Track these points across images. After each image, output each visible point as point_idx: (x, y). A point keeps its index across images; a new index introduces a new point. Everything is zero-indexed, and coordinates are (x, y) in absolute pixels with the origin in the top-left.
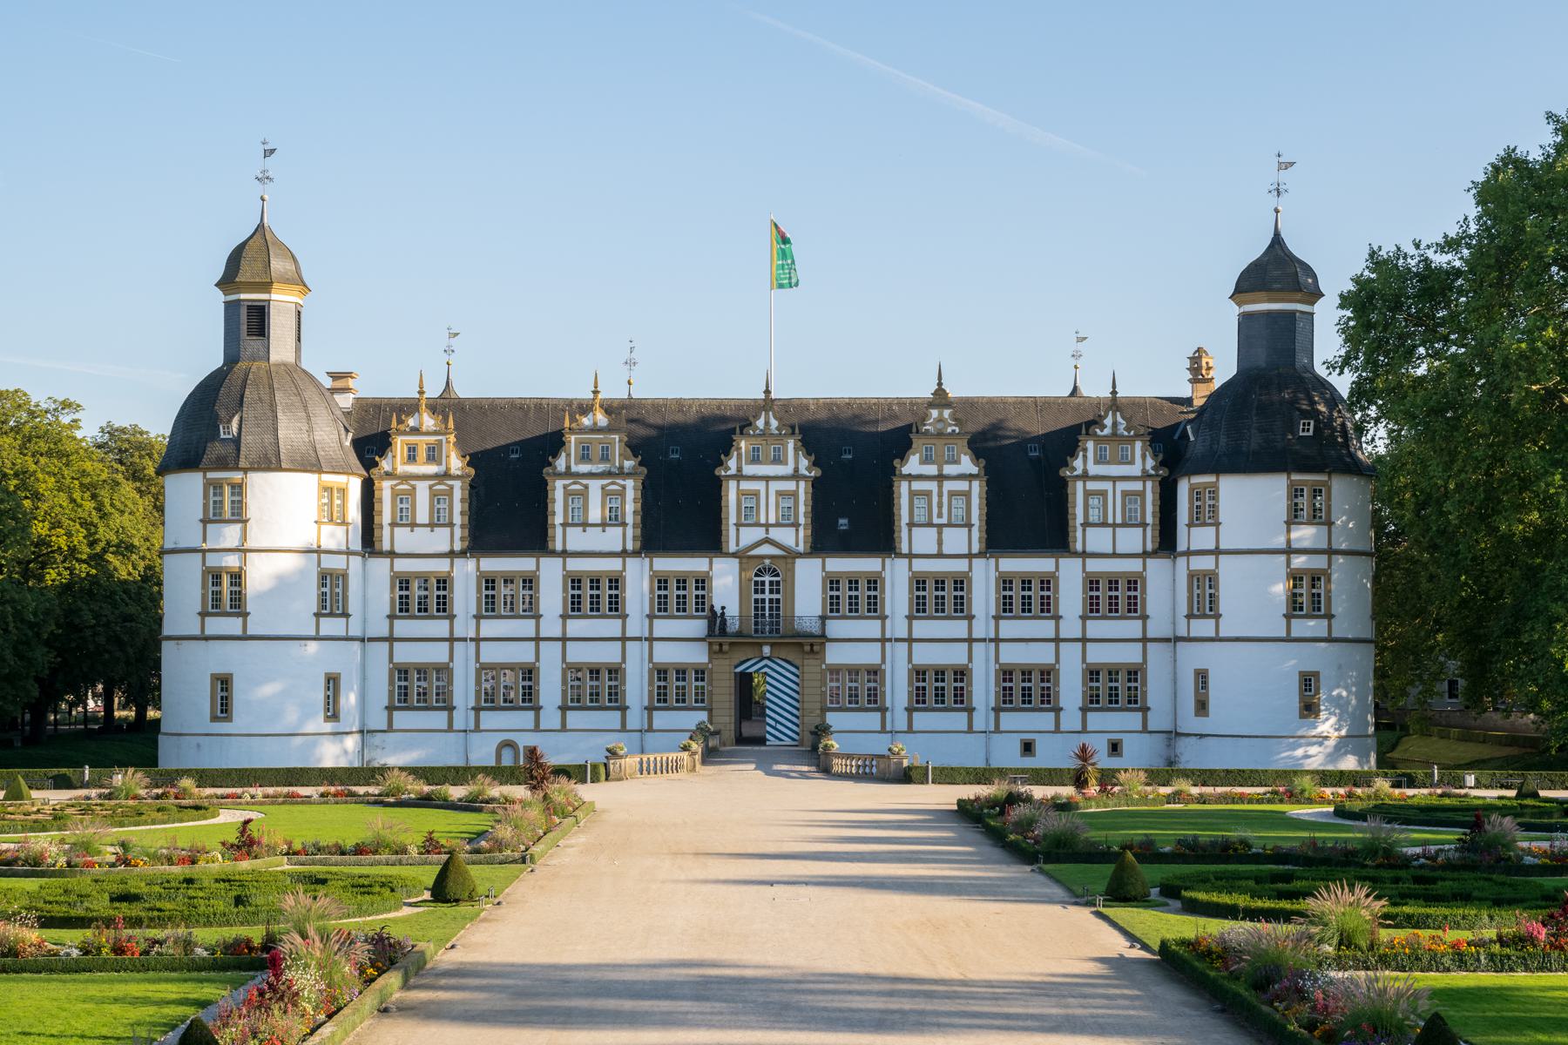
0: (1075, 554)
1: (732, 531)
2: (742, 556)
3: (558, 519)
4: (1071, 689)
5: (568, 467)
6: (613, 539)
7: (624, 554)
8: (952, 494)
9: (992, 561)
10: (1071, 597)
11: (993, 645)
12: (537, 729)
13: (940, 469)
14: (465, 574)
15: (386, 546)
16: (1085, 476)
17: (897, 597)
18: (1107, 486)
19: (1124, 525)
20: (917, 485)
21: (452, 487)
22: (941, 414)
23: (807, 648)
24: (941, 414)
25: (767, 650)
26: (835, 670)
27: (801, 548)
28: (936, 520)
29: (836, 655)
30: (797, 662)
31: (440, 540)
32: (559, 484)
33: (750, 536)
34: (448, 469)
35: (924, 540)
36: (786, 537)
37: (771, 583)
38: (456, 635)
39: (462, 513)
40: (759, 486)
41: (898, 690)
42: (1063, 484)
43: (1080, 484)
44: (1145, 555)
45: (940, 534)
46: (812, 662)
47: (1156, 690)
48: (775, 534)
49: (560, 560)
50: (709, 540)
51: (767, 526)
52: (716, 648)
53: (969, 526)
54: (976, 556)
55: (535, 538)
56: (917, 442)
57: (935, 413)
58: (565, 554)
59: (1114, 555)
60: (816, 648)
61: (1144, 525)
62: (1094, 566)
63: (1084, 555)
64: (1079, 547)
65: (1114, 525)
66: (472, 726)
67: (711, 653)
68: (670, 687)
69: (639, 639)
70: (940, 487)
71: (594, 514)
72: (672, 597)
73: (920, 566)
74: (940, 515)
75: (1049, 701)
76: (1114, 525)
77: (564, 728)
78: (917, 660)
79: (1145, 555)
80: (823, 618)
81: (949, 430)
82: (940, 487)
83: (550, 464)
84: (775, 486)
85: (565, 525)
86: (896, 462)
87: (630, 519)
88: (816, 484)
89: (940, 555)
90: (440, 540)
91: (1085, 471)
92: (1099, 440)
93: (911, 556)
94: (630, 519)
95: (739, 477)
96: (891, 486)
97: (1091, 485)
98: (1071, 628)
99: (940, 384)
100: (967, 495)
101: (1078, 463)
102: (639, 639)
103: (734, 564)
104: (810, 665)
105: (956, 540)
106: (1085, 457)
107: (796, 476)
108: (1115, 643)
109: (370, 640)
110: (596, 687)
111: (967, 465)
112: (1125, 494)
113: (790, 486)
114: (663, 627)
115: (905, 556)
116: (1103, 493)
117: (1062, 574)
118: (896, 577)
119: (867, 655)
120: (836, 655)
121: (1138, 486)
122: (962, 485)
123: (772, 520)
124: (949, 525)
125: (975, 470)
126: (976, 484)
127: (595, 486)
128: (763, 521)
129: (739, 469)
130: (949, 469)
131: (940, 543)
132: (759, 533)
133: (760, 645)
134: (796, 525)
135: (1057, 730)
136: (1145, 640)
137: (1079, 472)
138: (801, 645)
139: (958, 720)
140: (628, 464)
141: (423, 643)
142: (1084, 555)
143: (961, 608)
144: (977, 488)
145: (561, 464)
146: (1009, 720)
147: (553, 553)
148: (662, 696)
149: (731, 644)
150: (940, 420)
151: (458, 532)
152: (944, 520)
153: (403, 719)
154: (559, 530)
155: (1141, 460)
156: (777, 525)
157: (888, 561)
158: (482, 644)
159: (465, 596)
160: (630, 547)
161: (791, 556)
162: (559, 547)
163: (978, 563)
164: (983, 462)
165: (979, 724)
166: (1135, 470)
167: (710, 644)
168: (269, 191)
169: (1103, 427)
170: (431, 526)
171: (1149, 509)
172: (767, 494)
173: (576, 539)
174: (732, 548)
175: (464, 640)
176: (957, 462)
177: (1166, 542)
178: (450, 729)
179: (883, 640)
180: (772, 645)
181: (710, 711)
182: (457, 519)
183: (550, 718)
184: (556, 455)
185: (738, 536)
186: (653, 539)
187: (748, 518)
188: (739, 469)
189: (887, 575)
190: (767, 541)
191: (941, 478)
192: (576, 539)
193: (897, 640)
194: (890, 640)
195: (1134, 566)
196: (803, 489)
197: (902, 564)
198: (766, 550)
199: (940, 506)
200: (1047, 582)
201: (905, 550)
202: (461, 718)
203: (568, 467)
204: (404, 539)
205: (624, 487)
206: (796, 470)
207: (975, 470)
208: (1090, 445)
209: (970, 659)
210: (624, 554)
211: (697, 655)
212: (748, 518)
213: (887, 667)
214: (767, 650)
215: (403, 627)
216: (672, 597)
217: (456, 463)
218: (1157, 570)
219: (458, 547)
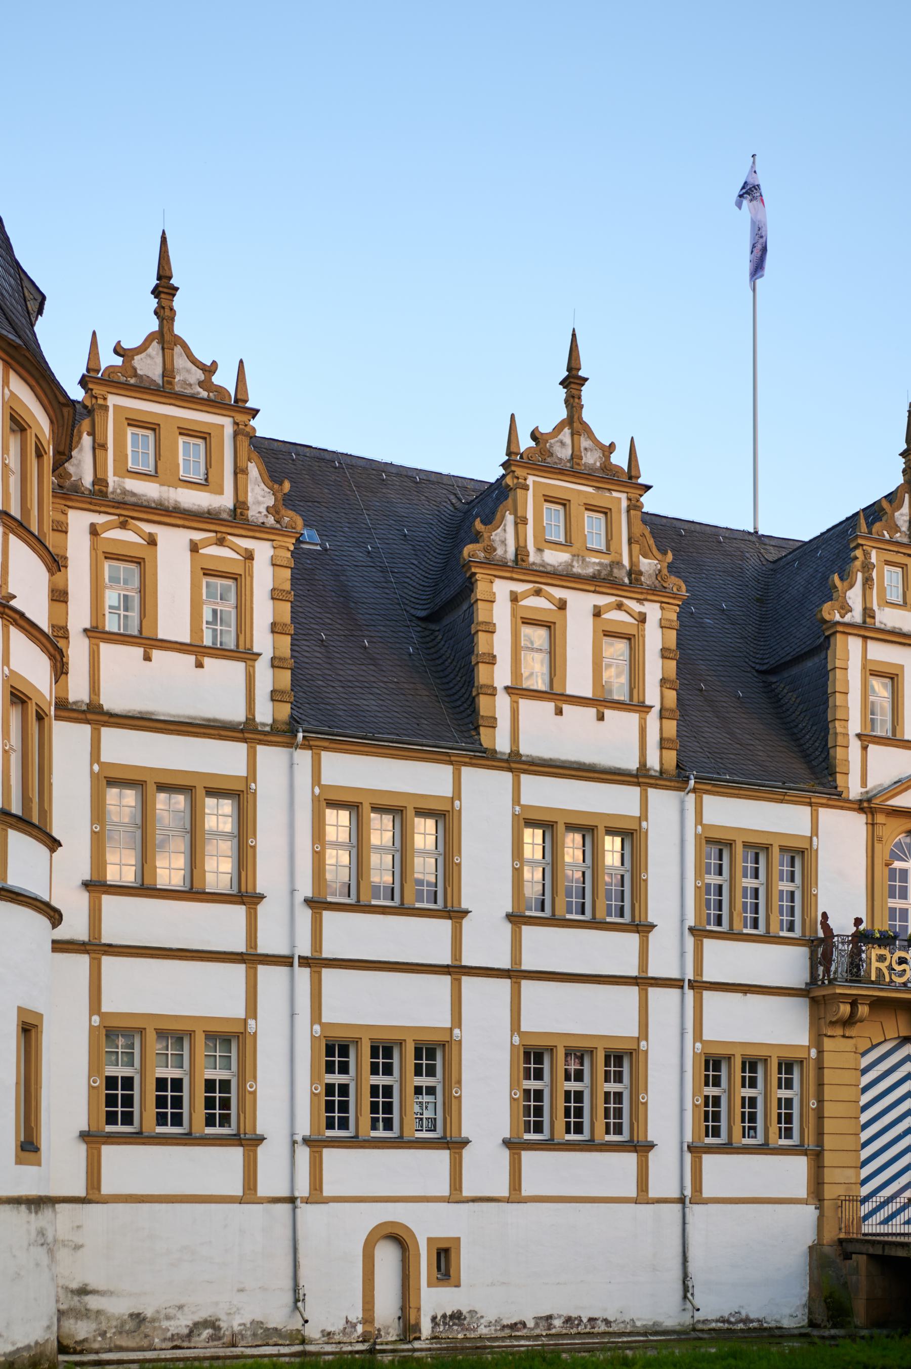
2: (866, 806)
6: (619, 740)
7: (640, 778)
32: (502, 589)
38: (264, 947)
49: (506, 778)
58: (517, 764)
69: (675, 983)
72: (747, 891)
83: (476, 538)
85: (515, 691)
94: (652, 696)
102: (675, 983)
103: (857, 823)
110: (575, 1096)
114: (725, 960)
127: (581, 604)
129: (868, 612)
147: (487, 758)
151: (265, 678)
154: (503, 703)
160: (653, 762)
162: (503, 745)
167: (815, 1003)
173: (541, 731)
175: (285, 961)
210: (640, 778)
211: (782, 1027)
216: (747, 891)
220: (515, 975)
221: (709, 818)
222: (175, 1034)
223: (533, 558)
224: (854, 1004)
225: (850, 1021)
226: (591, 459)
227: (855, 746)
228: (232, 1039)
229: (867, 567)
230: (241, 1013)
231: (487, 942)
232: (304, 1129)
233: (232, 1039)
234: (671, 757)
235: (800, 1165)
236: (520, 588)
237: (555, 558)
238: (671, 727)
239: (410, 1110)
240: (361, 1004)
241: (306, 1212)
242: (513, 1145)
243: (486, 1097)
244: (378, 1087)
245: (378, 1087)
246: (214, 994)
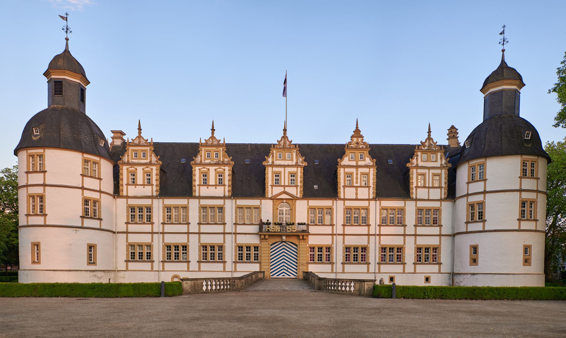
0: (412, 199)
1: (270, 188)
3: (197, 183)
4: (410, 255)
5: (201, 161)
6: (220, 191)
7: (224, 198)
8: (362, 174)
9: (378, 202)
10: (410, 218)
12: (188, 270)
13: (357, 163)
14: (158, 206)
15: (125, 193)
16: (417, 167)
17: (339, 217)
18: (426, 171)
19: (433, 187)
20: (348, 170)
21: (152, 169)
22: (357, 140)
23: (301, 237)
24: (357, 140)
25: (284, 238)
26: (312, 248)
27: (299, 196)
28: (355, 185)
29: (313, 241)
30: (297, 243)
31: (148, 191)
33: (277, 190)
34: (151, 161)
35: (350, 193)
36: (292, 191)
37: (286, 210)
39: (156, 180)
40: (281, 169)
41: (338, 255)
42: (408, 170)
43: (415, 170)
44: (441, 200)
45: (357, 190)
46: (303, 243)
47: (445, 256)
48: (288, 189)
50: (261, 193)
51: (284, 186)
52: (263, 237)
53: (369, 187)
54: (371, 200)
55: (187, 191)
56: (347, 152)
57: (355, 139)
58: (200, 198)
59: (429, 200)
60: (305, 237)
61: (440, 187)
62: (421, 204)
63: (417, 200)
64: (414, 197)
65: (429, 188)
66: (161, 269)
67: (261, 239)
68: (245, 253)
70: (357, 171)
71: (212, 181)
73: (349, 204)
74: (357, 183)
75: (400, 259)
76: (429, 188)
77: (199, 270)
79: (441, 200)
81: (361, 147)
82: (357, 171)
84: (288, 170)
86: (339, 160)
87: (227, 183)
88: (305, 169)
89: (357, 199)
90: (148, 191)
91: (417, 165)
92: (424, 152)
93: (344, 199)
94: (227, 183)
95: (273, 165)
96: (337, 170)
97: (420, 171)
98: (410, 230)
99: (357, 127)
100: (368, 174)
101: (414, 161)
103: (271, 202)
104: (302, 244)
105: (364, 193)
106: (417, 158)
107: (296, 165)
108: (429, 237)
109: (118, 233)
110: (212, 253)
111: (368, 161)
112: (434, 175)
113: (294, 170)
115: (342, 199)
116: (424, 175)
117: (407, 208)
118: (339, 207)
119: (325, 241)
120: (313, 241)
121: (438, 171)
122: (366, 170)
123: (287, 184)
124: (361, 187)
125: (371, 164)
126: (372, 170)
127: (212, 169)
128: (283, 184)
129: (273, 162)
130: (360, 163)
131: (357, 194)
132: (281, 189)
133: (281, 236)
134: (297, 186)
135: (404, 272)
136: (440, 235)
137: (414, 165)
138: (298, 236)
140: (226, 160)
141: (140, 235)
142: (417, 200)
143: (365, 222)
144: (372, 172)
145: (198, 159)
146: (384, 268)
147: (195, 197)
148: (241, 257)
149: (269, 235)
150: (357, 143)
151: (155, 188)
152: (359, 185)
153: (132, 266)
154: (197, 188)
155: (439, 160)
156: (288, 186)
157: (335, 202)
158: (165, 235)
159: (158, 215)
160: (227, 194)
161: (294, 198)
163: (372, 203)
164: (375, 160)
165: (372, 269)
166: (438, 164)
167: (260, 235)
169: (424, 146)
170: (144, 185)
171: (443, 181)
172: (283, 174)
173: (204, 191)
174: (270, 195)
176: (364, 160)
177: (451, 193)
178: (152, 270)
179: (332, 235)
180: (287, 236)
181: (260, 263)
182: (154, 182)
183: (194, 265)
184: (196, 156)
185: (272, 191)
186: (237, 192)
187: (277, 183)
188: (273, 162)
189: (334, 207)
190: (285, 192)
191: (357, 167)
192: (204, 191)
194: (335, 235)
195: (436, 204)
196: (299, 172)
197: (340, 203)
198: (284, 196)
199: (357, 179)
200: (402, 210)
201: (342, 197)
202: (156, 266)
203: (201, 161)
204: (132, 191)
205: (224, 170)
206: (297, 163)
207: (371, 164)
208: (419, 154)
209: (369, 243)
210: (224, 198)
211: (254, 240)
212: (277, 183)
213: (334, 246)
214: (284, 238)
215: (132, 228)
217: (154, 159)
218: (446, 207)
219: (155, 194)
220: (199, 233)
221: (237, 204)
222: (141, 246)
223: (203, 162)
224: (265, 236)
225: (265, 239)
226: (215, 143)
227: (270, 188)
228: (149, 246)
229: (273, 154)
230: (150, 241)
231: (194, 228)
232: (161, 260)
233: (149, 246)
234: (230, 193)
235: (258, 265)
236: (200, 167)
237: (207, 161)
238: (230, 188)
239: (181, 256)
240: (171, 239)
241: (162, 273)
242: (199, 262)
243: (194, 254)
244: (176, 253)
245: (176, 253)
246: (146, 239)
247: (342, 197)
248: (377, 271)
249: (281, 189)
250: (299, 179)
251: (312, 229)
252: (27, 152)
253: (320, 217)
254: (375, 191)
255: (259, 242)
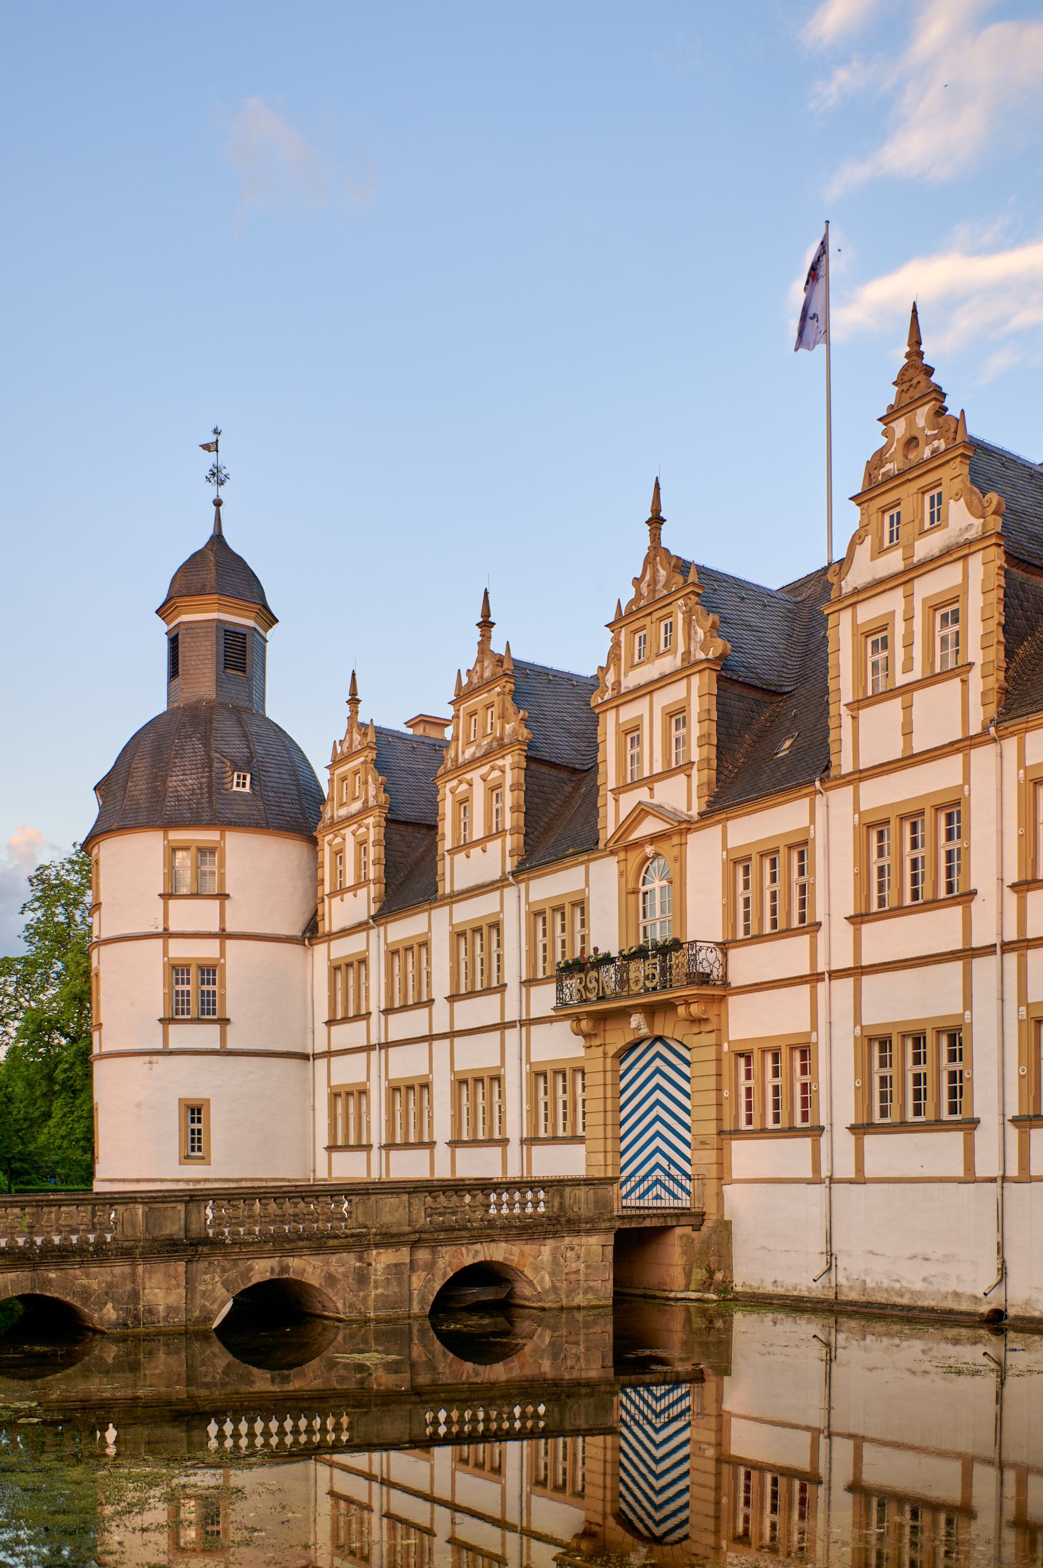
11: (1011, 960)
29: (749, 1020)
33: (629, 801)
78: (874, 1016)
80: (724, 947)
107: (688, 668)
139: (943, 1151)
165: (987, 1164)
168: (224, 492)
193: (835, 974)
214: (636, 1020)
247: (847, 767)
248: (1013, 1171)
249: (642, 794)
250: (695, 730)
251: (747, 965)
252: (165, 837)
253: (775, 897)
254: (831, 684)
255: (582, 1053)
